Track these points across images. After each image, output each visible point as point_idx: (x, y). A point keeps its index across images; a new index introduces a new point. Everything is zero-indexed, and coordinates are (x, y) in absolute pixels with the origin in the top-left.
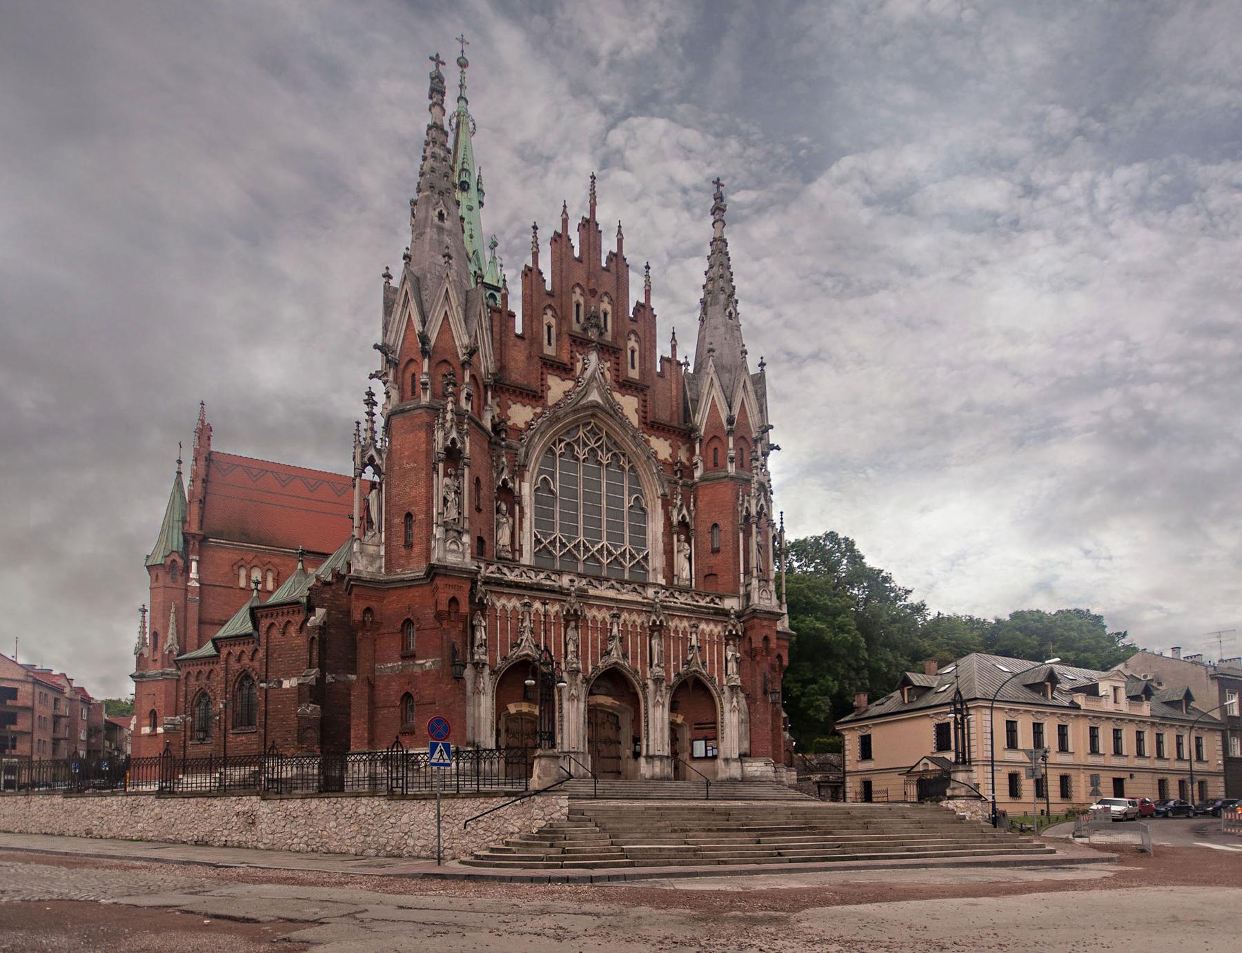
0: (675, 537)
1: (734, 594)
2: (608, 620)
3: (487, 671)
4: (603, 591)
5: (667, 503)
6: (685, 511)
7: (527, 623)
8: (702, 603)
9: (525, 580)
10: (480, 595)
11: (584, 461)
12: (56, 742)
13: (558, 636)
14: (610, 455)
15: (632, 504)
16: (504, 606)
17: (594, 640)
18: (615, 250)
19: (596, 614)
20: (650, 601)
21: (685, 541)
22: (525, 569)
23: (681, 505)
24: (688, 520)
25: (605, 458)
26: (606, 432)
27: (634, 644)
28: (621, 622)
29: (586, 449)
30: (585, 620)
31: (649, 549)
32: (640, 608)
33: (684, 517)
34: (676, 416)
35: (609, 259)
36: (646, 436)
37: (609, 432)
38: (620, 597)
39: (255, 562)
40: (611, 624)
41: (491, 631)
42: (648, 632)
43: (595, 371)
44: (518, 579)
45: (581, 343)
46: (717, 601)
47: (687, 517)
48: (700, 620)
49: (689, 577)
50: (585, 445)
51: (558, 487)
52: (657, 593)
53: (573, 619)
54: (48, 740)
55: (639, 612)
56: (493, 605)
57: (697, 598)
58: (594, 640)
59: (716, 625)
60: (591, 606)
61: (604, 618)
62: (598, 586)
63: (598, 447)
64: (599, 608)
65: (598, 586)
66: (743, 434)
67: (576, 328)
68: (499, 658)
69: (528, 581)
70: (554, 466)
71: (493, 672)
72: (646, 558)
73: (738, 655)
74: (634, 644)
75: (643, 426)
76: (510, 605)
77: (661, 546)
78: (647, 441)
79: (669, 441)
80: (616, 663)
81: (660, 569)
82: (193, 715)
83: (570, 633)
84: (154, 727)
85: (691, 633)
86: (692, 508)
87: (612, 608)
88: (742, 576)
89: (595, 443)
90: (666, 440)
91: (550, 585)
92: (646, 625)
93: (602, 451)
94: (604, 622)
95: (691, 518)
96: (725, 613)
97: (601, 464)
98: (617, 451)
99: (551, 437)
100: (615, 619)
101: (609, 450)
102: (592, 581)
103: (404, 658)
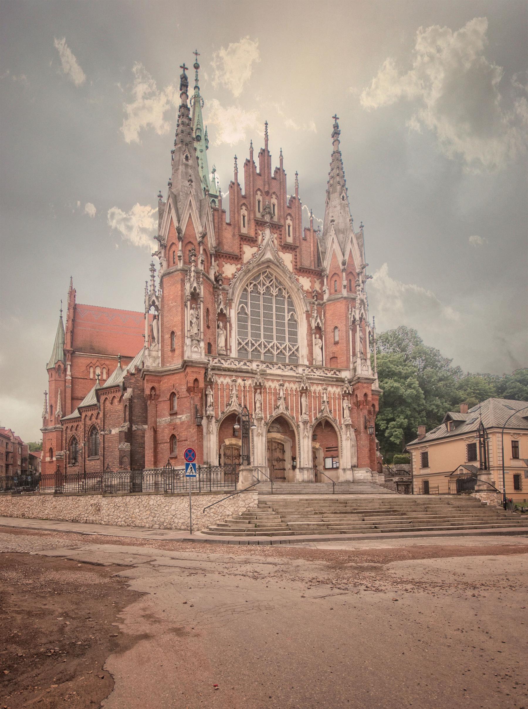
1: (347, 368)
2: (278, 387)
3: (214, 420)
4: (275, 371)
5: (309, 315)
6: (319, 320)
7: (234, 392)
8: (329, 375)
9: (233, 366)
10: (210, 376)
12: (7, 466)
13: (250, 398)
14: (277, 289)
17: (270, 400)
18: (279, 166)
20: (301, 376)
22: (233, 360)
23: (317, 317)
25: (274, 292)
27: (292, 401)
28: (285, 388)
29: (265, 287)
30: (265, 388)
32: (295, 379)
33: (318, 324)
34: (313, 263)
35: (276, 172)
36: (297, 277)
40: (279, 390)
41: (216, 398)
42: (299, 394)
43: (269, 240)
44: (229, 366)
45: (261, 224)
46: (337, 373)
48: (328, 385)
50: (264, 285)
51: (250, 309)
52: (304, 370)
53: (259, 387)
54: (4, 465)
55: (294, 382)
56: (217, 382)
57: (326, 372)
58: (270, 400)
60: (268, 380)
61: (275, 387)
62: (272, 368)
63: (271, 285)
64: (273, 380)
65: (272, 368)
66: (351, 270)
67: (259, 215)
68: (220, 413)
69: (235, 367)
70: (247, 299)
71: (217, 421)
73: (350, 406)
74: (292, 401)
75: (295, 271)
76: (225, 382)
78: (297, 280)
79: (310, 278)
80: (282, 413)
82: (69, 450)
83: (258, 396)
84: (52, 457)
86: (323, 318)
87: (279, 381)
88: (351, 357)
89: (269, 283)
91: (246, 369)
92: (298, 390)
93: (273, 287)
94: (275, 389)
95: (322, 324)
96: (342, 380)
97: (272, 295)
98: (281, 287)
99: (246, 282)
100: (281, 387)
101: (276, 287)
102: (269, 365)
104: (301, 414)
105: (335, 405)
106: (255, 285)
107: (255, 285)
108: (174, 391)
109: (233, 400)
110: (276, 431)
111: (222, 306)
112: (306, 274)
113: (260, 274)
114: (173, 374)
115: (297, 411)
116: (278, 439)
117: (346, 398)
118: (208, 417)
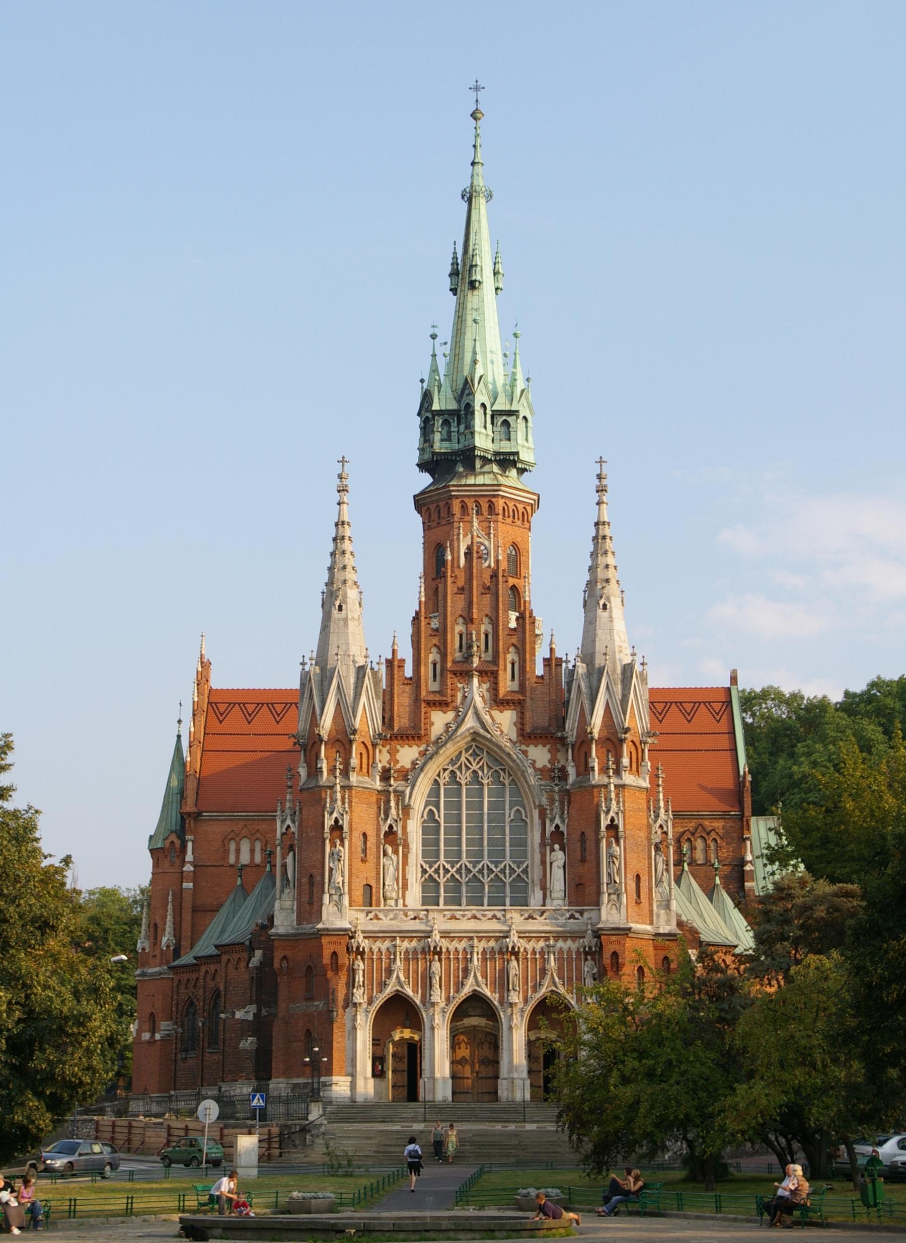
0: (548, 848)
6: (557, 821)
11: (466, 784)
15: (512, 817)
16: (379, 949)
19: (457, 945)
21: (560, 849)
24: (561, 829)
26: (487, 751)
29: (468, 773)
31: (528, 862)
33: (557, 827)
36: (524, 747)
37: (489, 751)
38: (479, 928)
39: (244, 832)
40: (472, 953)
46: (577, 915)
47: (561, 825)
48: (556, 939)
49: (563, 888)
50: (468, 768)
56: (371, 949)
59: (574, 941)
64: (460, 939)
70: (438, 796)
72: (525, 871)
75: (520, 738)
77: (537, 857)
78: (525, 753)
79: (548, 746)
81: (537, 881)
85: (548, 953)
86: (565, 816)
87: (471, 938)
89: (478, 763)
90: (544, 746)
97: (482, 784)
98: (497, 768)
101: (490, 768)
103: (307, 1000)
104: (509, 990)
105: (570, 970)
106: (452, 772)
107: (452, 772)
108: (310, 964)
109: (395, 975)
110: (479, 1013)
111: (389, 822)
112: (540, 741)
113: (461, 752)
114: (311, 939)
115: (502, 986)
116: (485, 1027)
117: (589, 957)
118: (355, 1004)
